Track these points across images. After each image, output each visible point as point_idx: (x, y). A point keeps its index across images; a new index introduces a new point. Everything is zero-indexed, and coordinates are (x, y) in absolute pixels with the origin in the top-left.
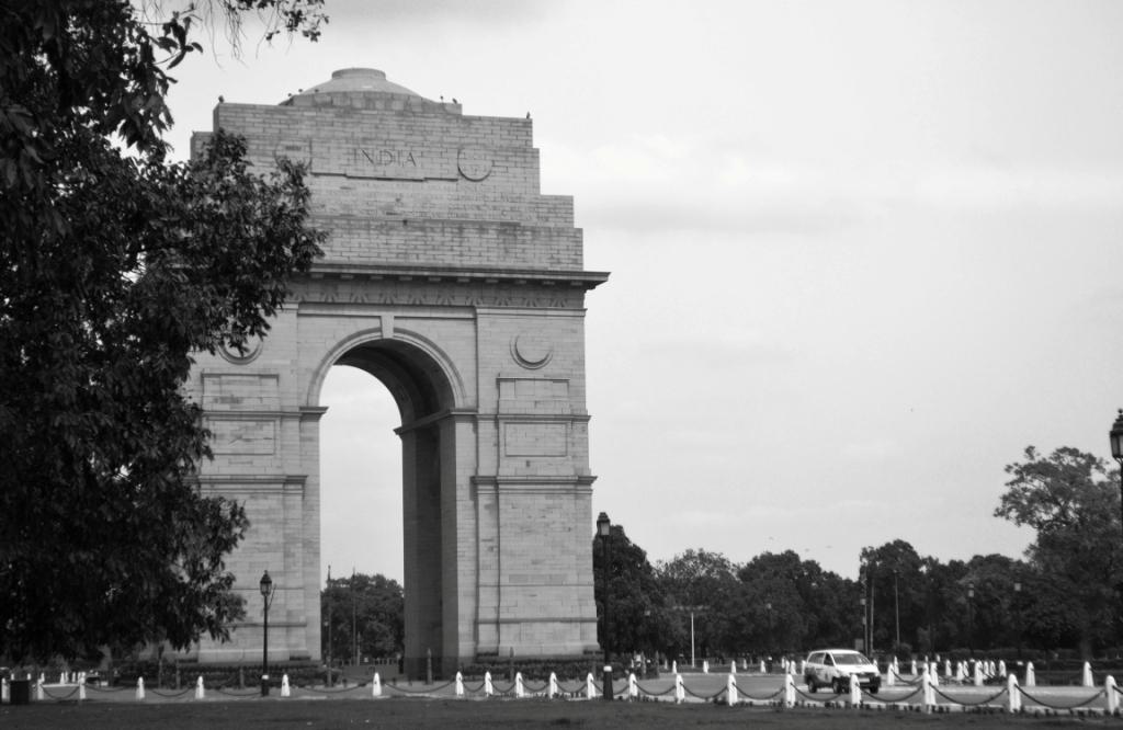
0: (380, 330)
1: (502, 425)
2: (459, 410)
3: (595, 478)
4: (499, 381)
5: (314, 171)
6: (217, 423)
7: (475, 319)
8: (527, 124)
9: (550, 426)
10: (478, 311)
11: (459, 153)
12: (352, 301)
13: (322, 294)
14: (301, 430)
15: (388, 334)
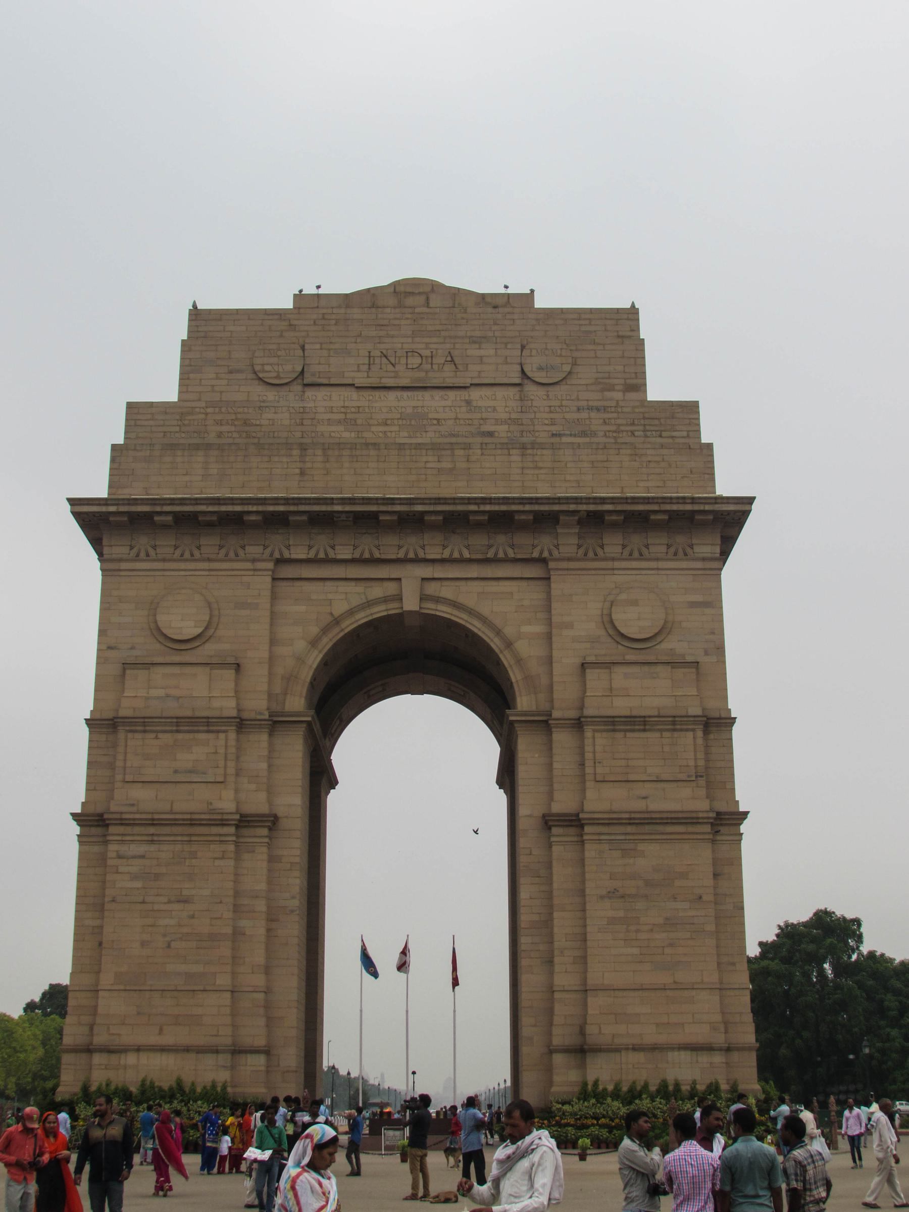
0: (399, 598)
1: (588, 734)
2: (525, 714)
3: (746, 814)
4: (583, 666)
5: (305, 382)
6: (139, 736)
7: (549, 578)
8: (632, 314)
9: (666, 734)
10: (552, 565)
11: (522, 351)
12: (357, 556)
13: (310, 547)
14: (271, 749)
15: (411, 604)
